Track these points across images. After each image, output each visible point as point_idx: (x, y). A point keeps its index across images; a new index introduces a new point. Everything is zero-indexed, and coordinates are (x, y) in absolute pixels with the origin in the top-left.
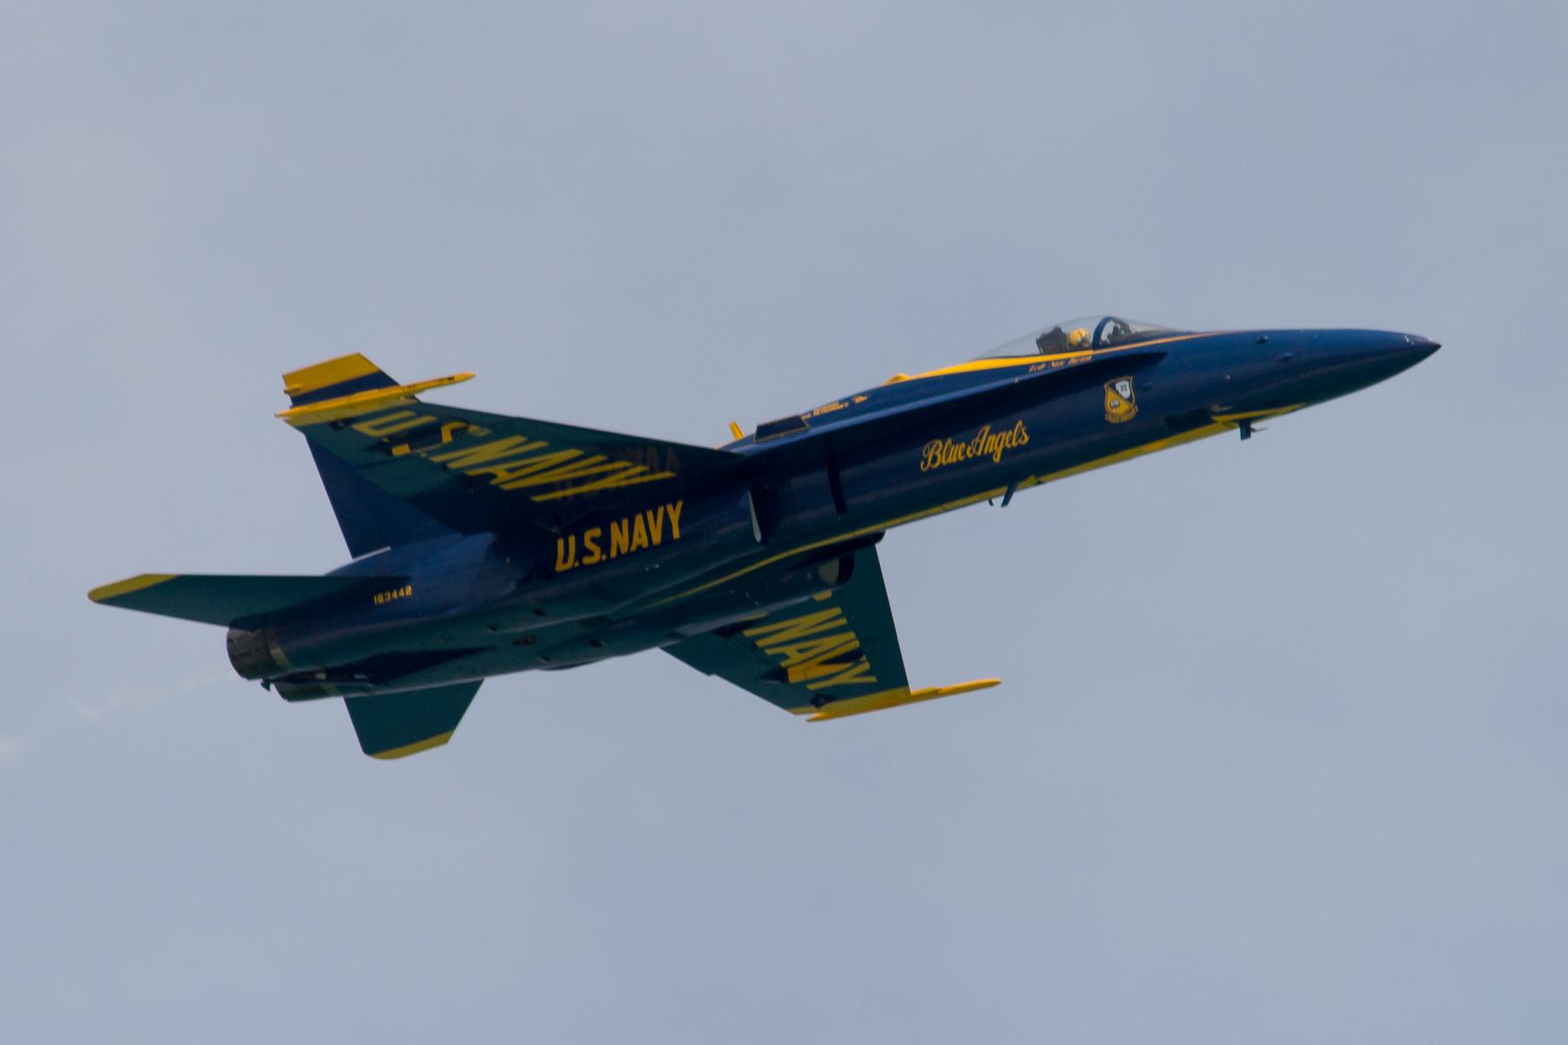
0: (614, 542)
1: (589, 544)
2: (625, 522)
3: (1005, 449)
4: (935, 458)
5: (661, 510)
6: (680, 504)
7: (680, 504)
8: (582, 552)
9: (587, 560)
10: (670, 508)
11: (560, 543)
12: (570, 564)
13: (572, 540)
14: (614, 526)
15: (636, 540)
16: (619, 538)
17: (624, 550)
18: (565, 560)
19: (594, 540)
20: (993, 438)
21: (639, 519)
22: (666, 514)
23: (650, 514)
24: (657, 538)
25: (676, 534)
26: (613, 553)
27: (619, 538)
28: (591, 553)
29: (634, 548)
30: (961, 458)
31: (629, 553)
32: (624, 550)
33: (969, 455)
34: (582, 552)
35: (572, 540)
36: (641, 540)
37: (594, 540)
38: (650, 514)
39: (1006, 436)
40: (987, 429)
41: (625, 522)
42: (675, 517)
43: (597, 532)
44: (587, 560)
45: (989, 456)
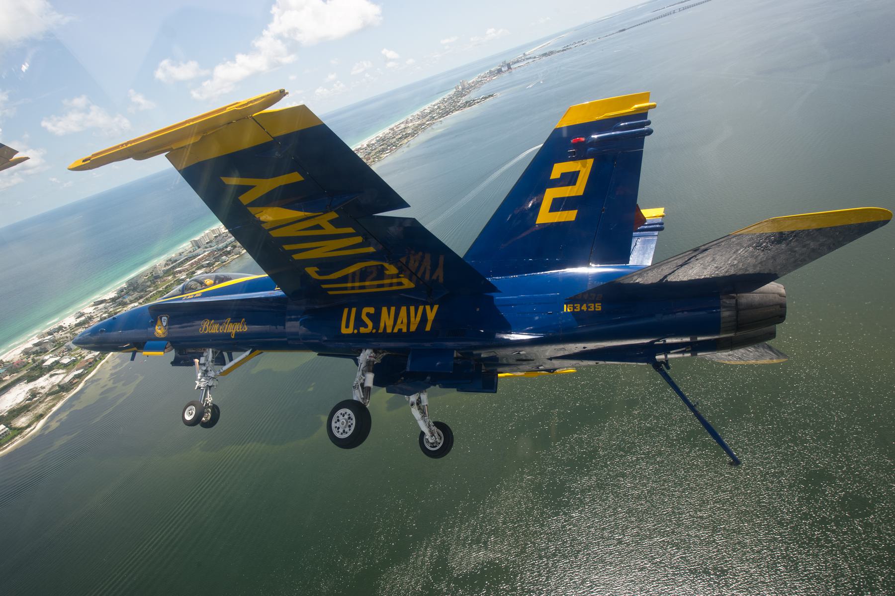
1: (364, 317)
2: (393, 309)
5: (421, 308)
6: (436, 307)
7: (436, 307)
8: (359, 323)
10: (428, 308)
11: (346, 311)
12: (350, 330)
13: (354, 310)
14: (384, 309)
16: (387, 320)
17: (389, 330)
18: (347, 326)
19: (368, 315)
21: (404, 310)
23: (412, 309)
25: (428, 328)
26: (381, 331)
27: (387, 320)
28: (366, 326)
29: (396, 330)
32: (389, 330)
34: (359, 323)
35: (354, 310)
37: (368, 315)
38: (412, 309)
41: (393, 309)
42: (431, 315)
43: (372, 310)
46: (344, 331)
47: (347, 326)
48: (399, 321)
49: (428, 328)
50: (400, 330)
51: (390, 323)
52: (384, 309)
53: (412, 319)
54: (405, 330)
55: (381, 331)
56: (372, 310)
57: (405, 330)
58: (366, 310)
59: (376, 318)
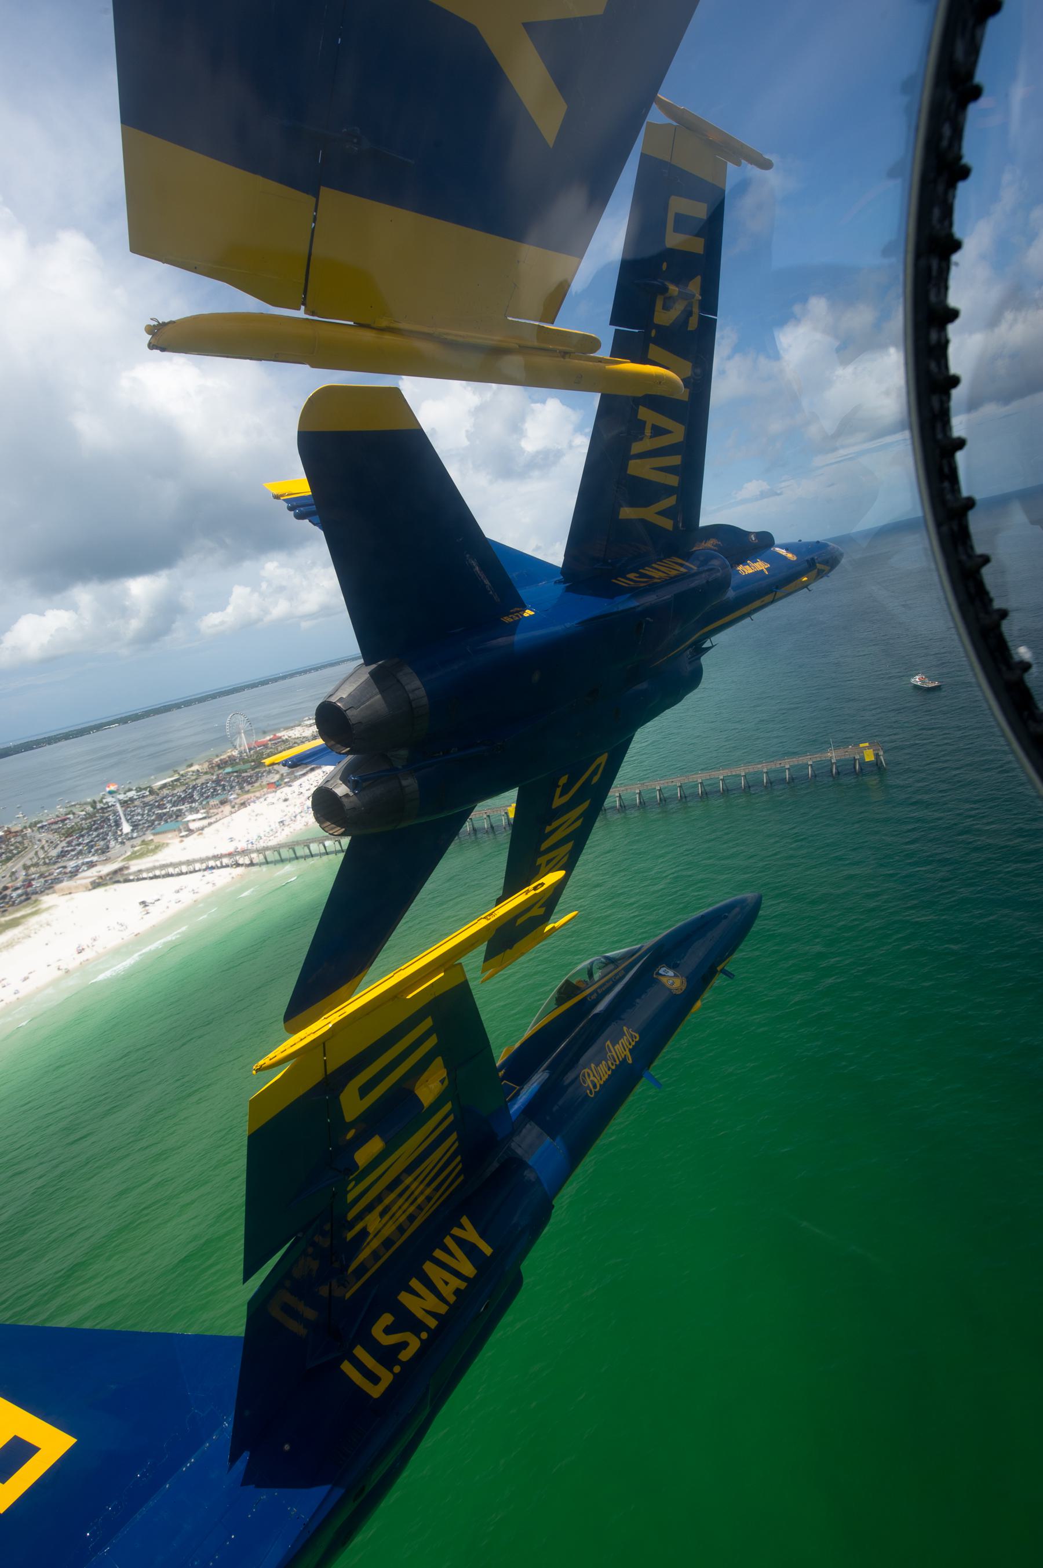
0: (420, 1314)
2: (414, 1283)
4: (592, 1081)
5: (448, 1241)
6: (465, 1221)
7: (465, 1221)
8: (387, 1356)
9: (405, 1356)
10: (456, 1231)
11: (347, 1367)
12: (387, 1378)
13: (360, 1352)
14: (404, 1298)
15: (448, 1292)
16: (420, 1303)
17: (443, 1309)
18: (375, 1379)
19: (388, 1330)
20: (617, 1047)
21: (429, 1267)
22: (461, 1242)
23: (438, 1254)
24: (468, 1269)
25: (488, 1250)
26: (432, 1323)
27: (420, 1303)
29: (452, 1299)
30: (609, 1073)
31: (452, 1307)
34: (387, 1356)
35: (360, 1352)
37: (388, 1330)
38: (438, 1254)
39: (624, 1041)
40: (608, 1043)
41: (414, 1283)
42: (470, 1233)
43: (387, 1319)
44: (405, 1356)
45: (625, 1059)
46: (376, 1391)
47: (375, 1379)
49: (488, 1250)
50: (457, 1292)
51: (431, 1302)
54: (462, 1285)
55: (432, 1323)
56: (387, 1319)
57: (462, 1285)
58: (377, 1331)
59: (406, 1321)
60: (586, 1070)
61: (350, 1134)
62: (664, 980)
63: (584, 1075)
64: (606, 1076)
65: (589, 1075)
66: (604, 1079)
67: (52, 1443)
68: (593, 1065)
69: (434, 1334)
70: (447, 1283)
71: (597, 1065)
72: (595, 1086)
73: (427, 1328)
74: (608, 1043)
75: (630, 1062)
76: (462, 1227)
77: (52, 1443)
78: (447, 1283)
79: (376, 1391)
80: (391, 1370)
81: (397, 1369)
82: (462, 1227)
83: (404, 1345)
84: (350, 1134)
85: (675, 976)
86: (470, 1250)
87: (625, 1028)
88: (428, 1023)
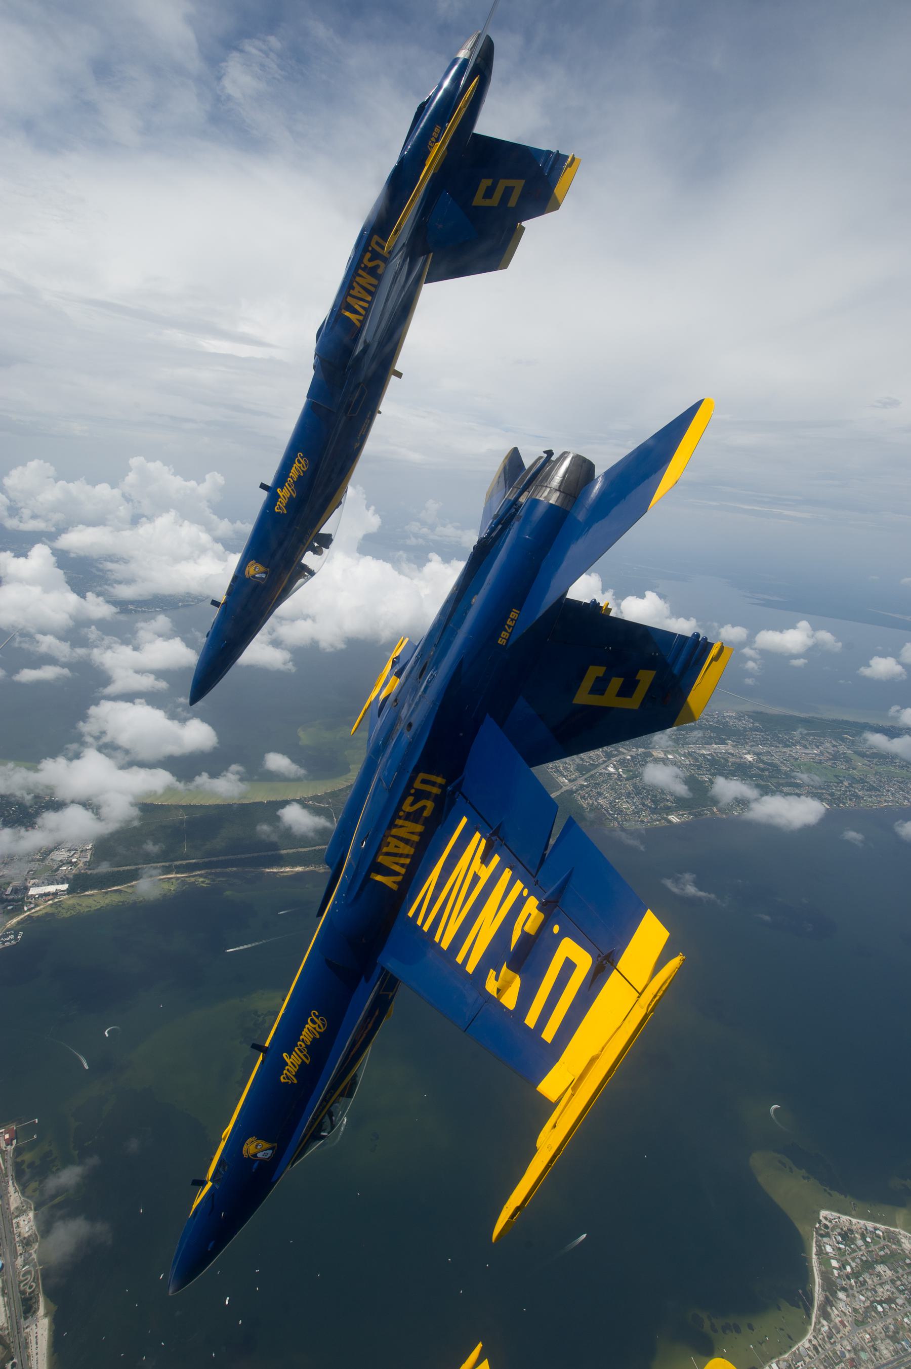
3: (287, 1064)
7: (395, 887)
9: (410, 799)
10: (399, 878)
12: (418, 785)
14: (419, 828)
17: (394, 831)
18: (424, 782)
19: (424, 807)
30: (301, 1037)
33: (299, 1043)
34: (420, 795)
36: (393, 845)
37: (424, 807)
39: (294, 1070)
43: (426, 813)
44: (410, 799)
45: (290, 1054)
46: (422, 776)
48: (402, 845)
52: (419, 828)
53: (397, 859)
56: (426, 813)
58: (430, 804)
60: (322, 1031)
61: (556, 929)
62: (266, 1145)
63: (324, 1025)
64: (303, 1033)
65: (320, 1027)
66: (306, 1030)
67: (583, 697)
68: (318, 1036)
69: (396, 816)
70: (396, 846)
71: (314, 1039)
72: (313, 1022)
73: (400, 818)
74: (308, 1062)
75: (285, 1055)
76: (394, 882)
77: (583, 697)
78: (396, 846)
79: (422, 776)
80: (416, 790)
81: (413, 791)
82: (394, 882)
83: (412, 804)
84: (556, 929)
85: (255, 1155)
86: (388, 872)
87: (296, 1081)
88: (548, 1035)
